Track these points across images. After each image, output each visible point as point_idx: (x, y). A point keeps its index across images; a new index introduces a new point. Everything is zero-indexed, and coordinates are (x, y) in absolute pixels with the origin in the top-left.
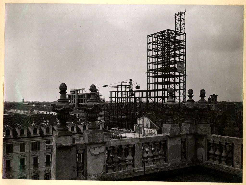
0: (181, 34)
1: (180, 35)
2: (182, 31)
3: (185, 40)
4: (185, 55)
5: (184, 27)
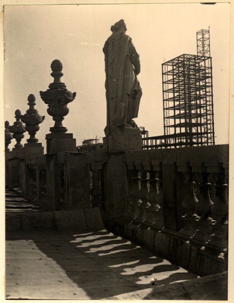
0: (206, 58)
1: (204, 60)
2: (207, 55)
3: (211, 66)
4: (212, 86)
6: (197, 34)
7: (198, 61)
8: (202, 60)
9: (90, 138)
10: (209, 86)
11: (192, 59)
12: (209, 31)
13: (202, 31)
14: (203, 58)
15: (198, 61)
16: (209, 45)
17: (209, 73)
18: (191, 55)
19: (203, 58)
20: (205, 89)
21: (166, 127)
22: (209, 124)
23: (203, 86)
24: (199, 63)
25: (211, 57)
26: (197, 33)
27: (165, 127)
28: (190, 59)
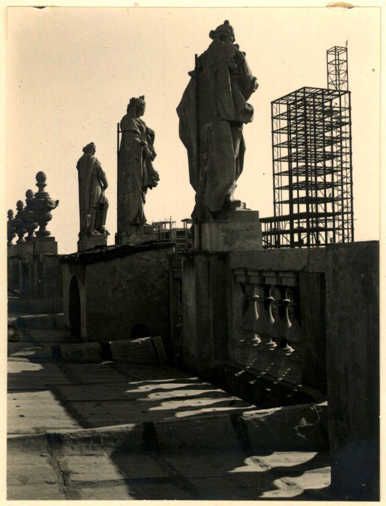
0: (341, 93)
1: (339, 96)
2: (344, 88)
4: (350, 138)
5: (346, 79)
6: (327, 53)
7: (329, 97)
8: (335, 95)
9: (163, 220)
10: (346, 138)
11: (319, 94)
12: (346, 48)
13: (334, 48)
14: (337, 93)
15: (329, 97)
16: (347, 72)
17: (345, 117)
18: (317, 89)
19: (337, 93)
20: (341, 142)
21: (277, 203)
22: (345, 199)
23: (337, 138)
24: (331, 100)
25: (349, 90)
26: (328, 52)
27: (275, 203)
28: (316, 94)
